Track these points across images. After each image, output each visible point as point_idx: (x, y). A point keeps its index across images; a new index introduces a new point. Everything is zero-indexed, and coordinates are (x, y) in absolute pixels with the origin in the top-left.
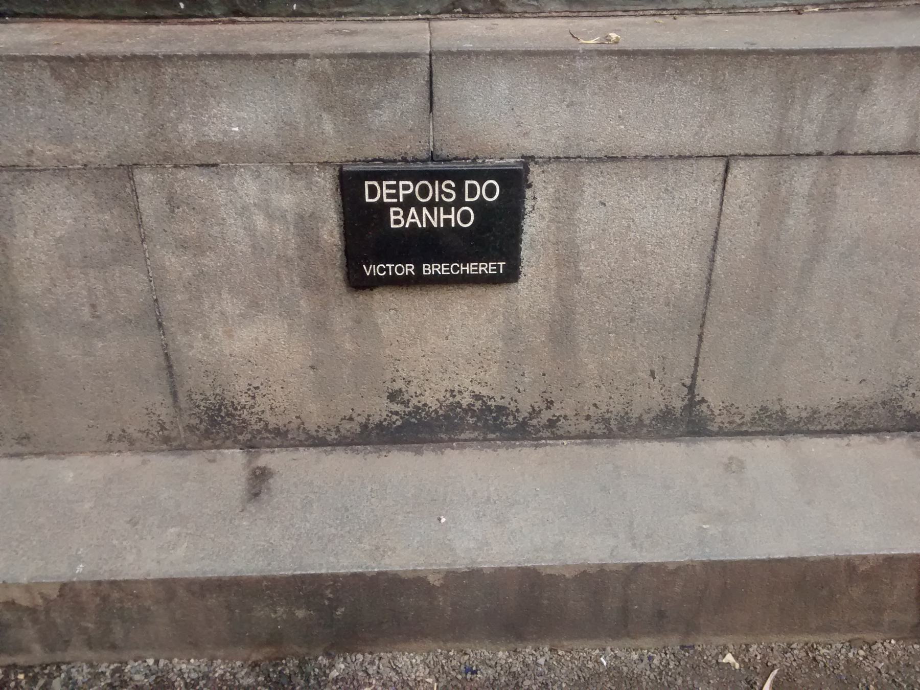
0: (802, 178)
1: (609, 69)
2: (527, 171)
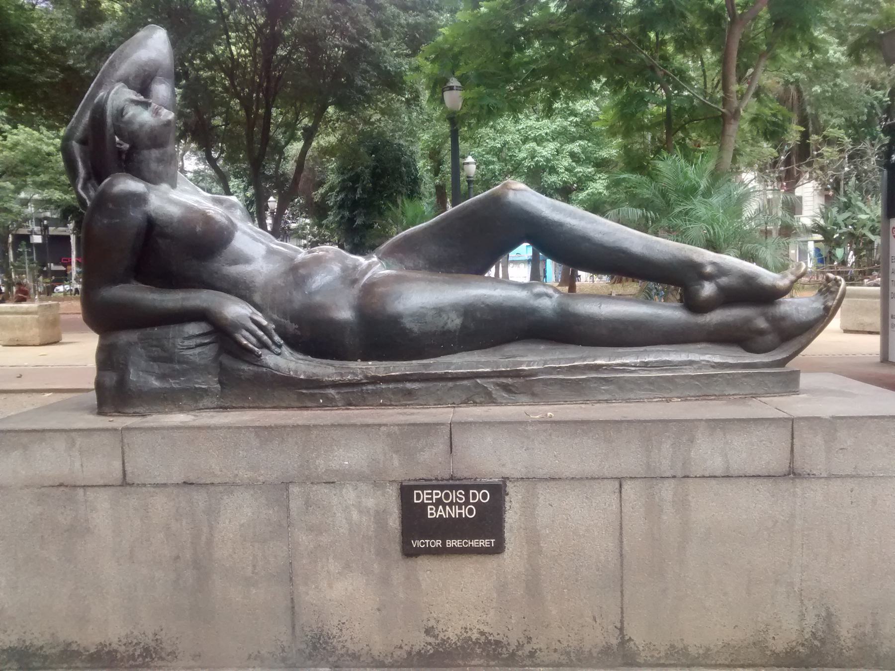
0: (667, 491)
1: (545, 431)
2: (506, 486)
